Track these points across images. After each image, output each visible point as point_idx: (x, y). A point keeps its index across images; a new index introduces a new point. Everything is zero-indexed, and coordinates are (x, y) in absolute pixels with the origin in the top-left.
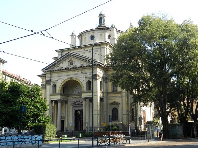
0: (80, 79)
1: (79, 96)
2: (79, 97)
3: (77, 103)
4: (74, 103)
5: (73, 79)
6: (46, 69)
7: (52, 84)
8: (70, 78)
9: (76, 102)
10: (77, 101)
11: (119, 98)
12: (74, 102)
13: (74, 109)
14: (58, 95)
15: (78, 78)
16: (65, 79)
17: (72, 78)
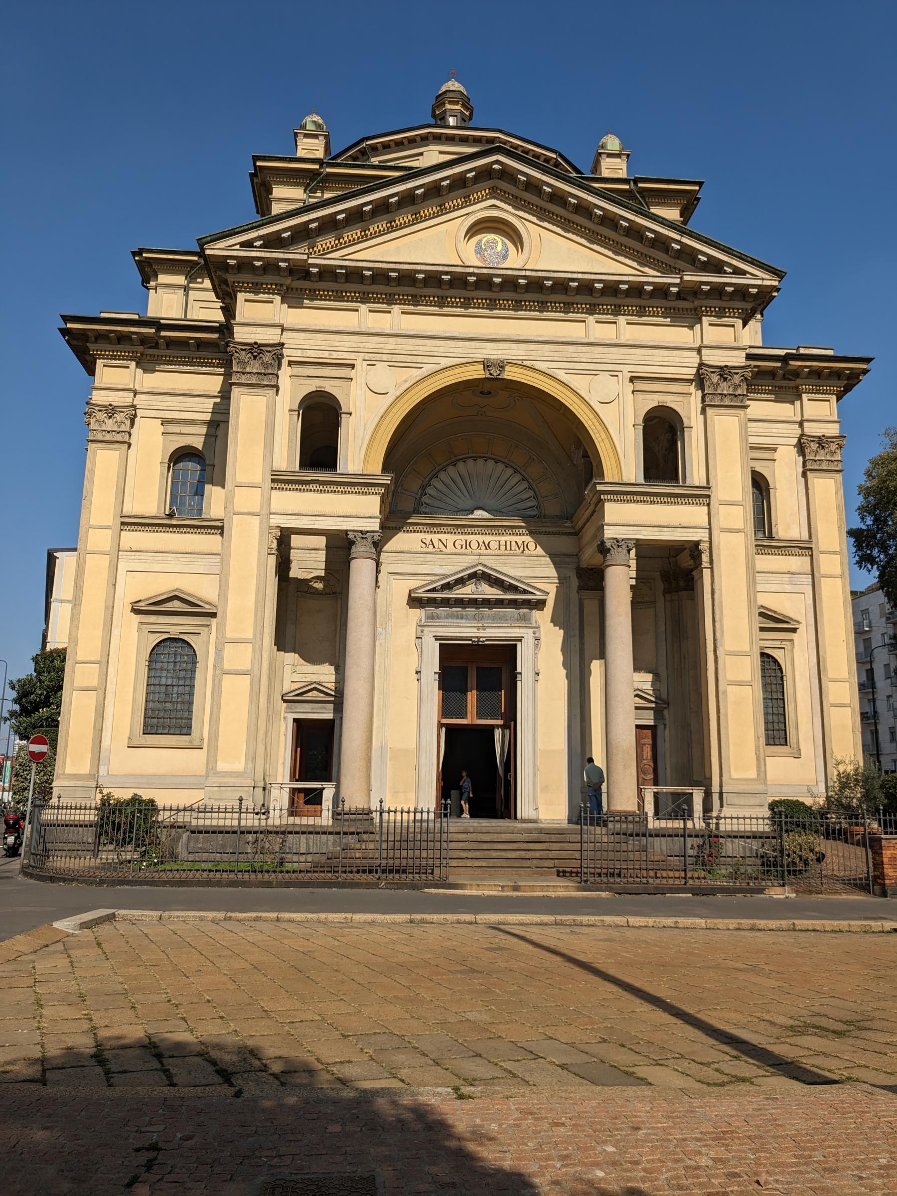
0: (576, 382)
1: (487, 539)
2: (487, 547)
3: (467, 591)
4: (448, 587)
5: (511, 374)
6: (248, 245)
7: (292, 388)
8: (487, 365)
9: (461, 582)
10: (473, 576)
11: (788, 588)
12: (446, 576)
13: (437, 638)
14: (358, 484)
15: (561, 375)
16: (427, 369)
17: (502, 365)
